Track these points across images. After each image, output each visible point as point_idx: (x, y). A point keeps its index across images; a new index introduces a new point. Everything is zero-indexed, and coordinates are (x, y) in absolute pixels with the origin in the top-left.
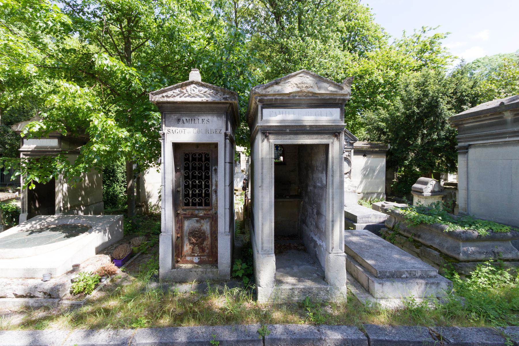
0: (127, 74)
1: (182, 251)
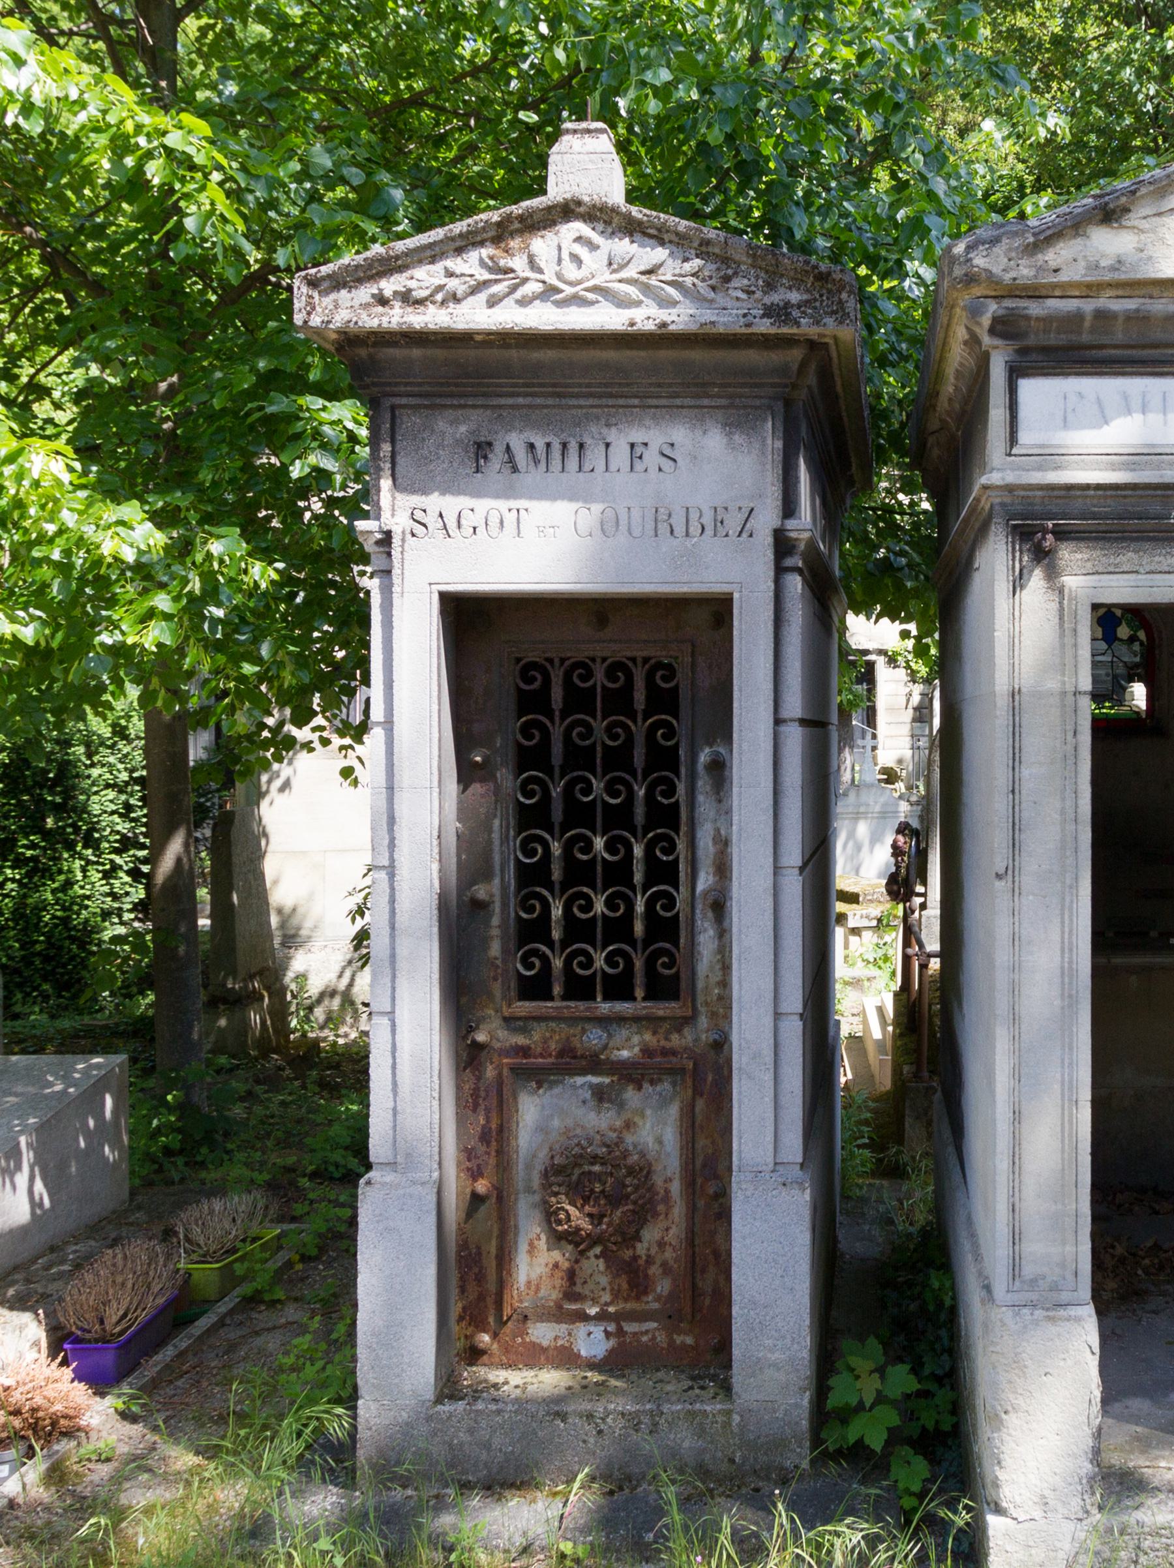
0: (149, 155)
1: (501, 1285)
